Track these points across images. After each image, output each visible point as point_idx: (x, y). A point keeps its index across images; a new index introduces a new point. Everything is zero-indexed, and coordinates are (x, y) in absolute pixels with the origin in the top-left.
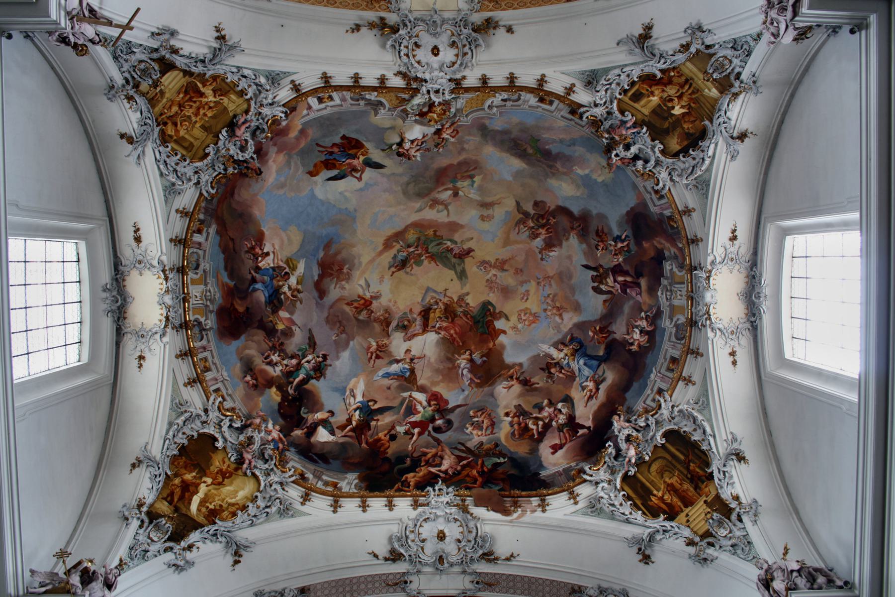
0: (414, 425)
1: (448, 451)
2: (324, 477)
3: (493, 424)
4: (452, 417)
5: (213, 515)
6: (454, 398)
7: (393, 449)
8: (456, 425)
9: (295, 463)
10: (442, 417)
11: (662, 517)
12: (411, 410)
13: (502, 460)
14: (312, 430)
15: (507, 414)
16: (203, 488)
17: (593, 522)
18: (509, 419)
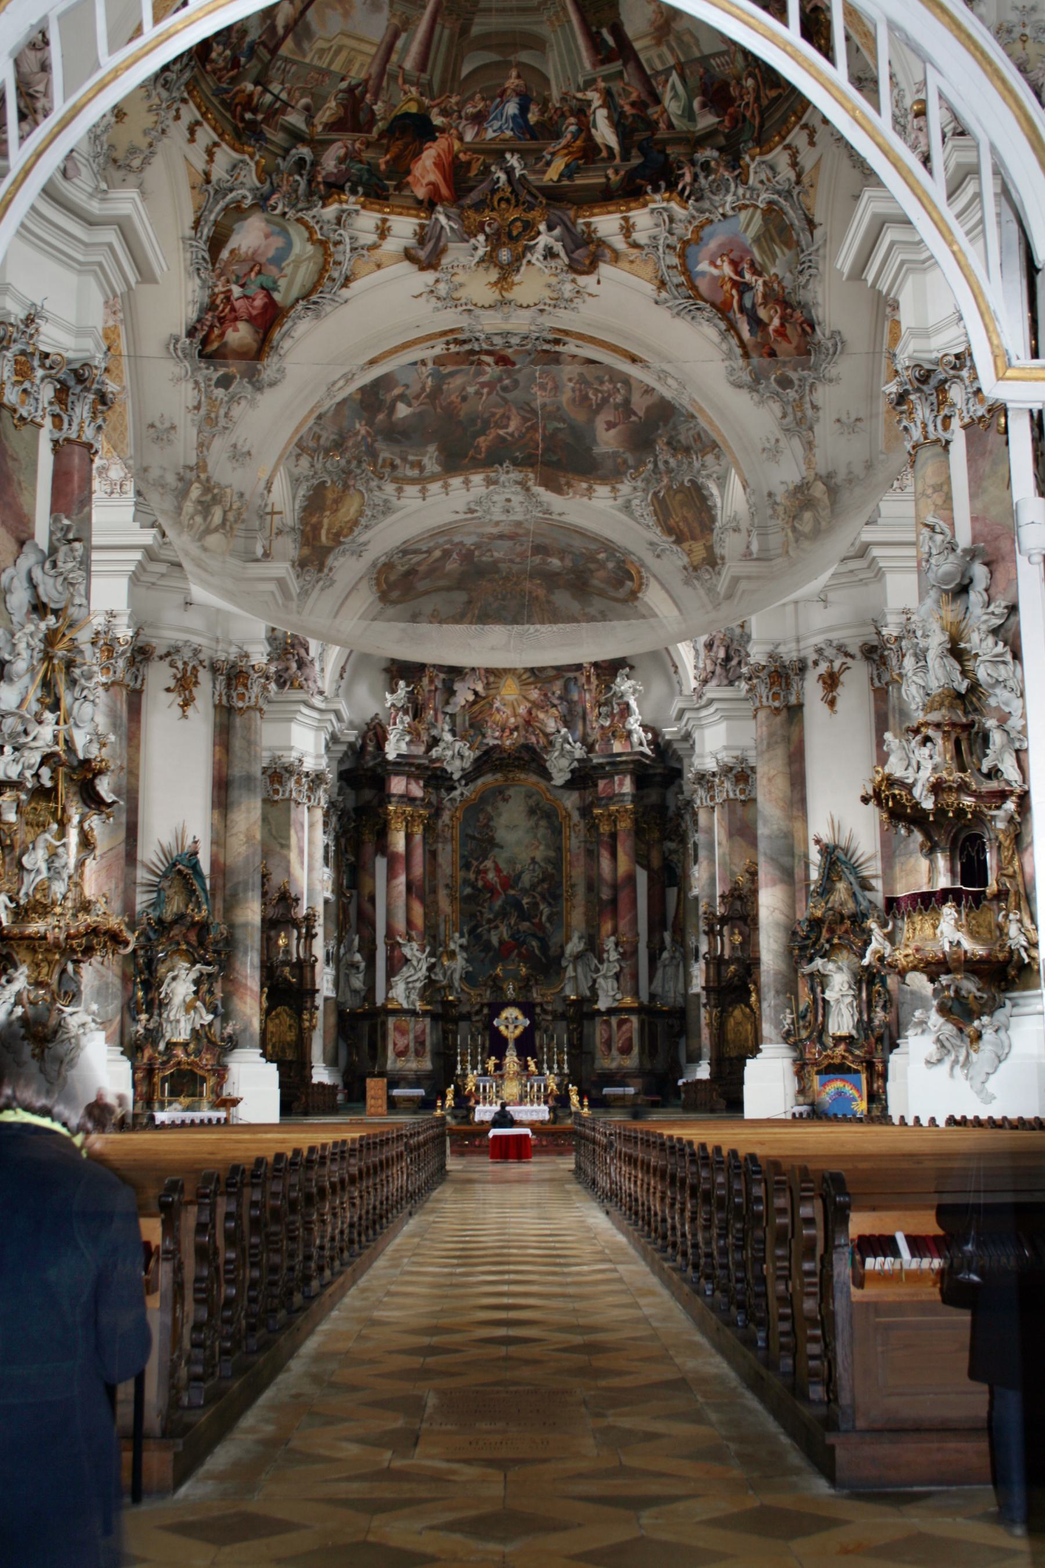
0: (483, 385)
1: (514, 411)
2: (411, 458)
5: (337, 537)
7: (464, 410)
8: (522, 384)
9: (385, 453)
10: (509, 376)
11: (673, 538)
13: (561, 425)
14: (392, 409)
15: (570, 380)
16: (326, 521)
17: (623, 517)
18: (571, 384)
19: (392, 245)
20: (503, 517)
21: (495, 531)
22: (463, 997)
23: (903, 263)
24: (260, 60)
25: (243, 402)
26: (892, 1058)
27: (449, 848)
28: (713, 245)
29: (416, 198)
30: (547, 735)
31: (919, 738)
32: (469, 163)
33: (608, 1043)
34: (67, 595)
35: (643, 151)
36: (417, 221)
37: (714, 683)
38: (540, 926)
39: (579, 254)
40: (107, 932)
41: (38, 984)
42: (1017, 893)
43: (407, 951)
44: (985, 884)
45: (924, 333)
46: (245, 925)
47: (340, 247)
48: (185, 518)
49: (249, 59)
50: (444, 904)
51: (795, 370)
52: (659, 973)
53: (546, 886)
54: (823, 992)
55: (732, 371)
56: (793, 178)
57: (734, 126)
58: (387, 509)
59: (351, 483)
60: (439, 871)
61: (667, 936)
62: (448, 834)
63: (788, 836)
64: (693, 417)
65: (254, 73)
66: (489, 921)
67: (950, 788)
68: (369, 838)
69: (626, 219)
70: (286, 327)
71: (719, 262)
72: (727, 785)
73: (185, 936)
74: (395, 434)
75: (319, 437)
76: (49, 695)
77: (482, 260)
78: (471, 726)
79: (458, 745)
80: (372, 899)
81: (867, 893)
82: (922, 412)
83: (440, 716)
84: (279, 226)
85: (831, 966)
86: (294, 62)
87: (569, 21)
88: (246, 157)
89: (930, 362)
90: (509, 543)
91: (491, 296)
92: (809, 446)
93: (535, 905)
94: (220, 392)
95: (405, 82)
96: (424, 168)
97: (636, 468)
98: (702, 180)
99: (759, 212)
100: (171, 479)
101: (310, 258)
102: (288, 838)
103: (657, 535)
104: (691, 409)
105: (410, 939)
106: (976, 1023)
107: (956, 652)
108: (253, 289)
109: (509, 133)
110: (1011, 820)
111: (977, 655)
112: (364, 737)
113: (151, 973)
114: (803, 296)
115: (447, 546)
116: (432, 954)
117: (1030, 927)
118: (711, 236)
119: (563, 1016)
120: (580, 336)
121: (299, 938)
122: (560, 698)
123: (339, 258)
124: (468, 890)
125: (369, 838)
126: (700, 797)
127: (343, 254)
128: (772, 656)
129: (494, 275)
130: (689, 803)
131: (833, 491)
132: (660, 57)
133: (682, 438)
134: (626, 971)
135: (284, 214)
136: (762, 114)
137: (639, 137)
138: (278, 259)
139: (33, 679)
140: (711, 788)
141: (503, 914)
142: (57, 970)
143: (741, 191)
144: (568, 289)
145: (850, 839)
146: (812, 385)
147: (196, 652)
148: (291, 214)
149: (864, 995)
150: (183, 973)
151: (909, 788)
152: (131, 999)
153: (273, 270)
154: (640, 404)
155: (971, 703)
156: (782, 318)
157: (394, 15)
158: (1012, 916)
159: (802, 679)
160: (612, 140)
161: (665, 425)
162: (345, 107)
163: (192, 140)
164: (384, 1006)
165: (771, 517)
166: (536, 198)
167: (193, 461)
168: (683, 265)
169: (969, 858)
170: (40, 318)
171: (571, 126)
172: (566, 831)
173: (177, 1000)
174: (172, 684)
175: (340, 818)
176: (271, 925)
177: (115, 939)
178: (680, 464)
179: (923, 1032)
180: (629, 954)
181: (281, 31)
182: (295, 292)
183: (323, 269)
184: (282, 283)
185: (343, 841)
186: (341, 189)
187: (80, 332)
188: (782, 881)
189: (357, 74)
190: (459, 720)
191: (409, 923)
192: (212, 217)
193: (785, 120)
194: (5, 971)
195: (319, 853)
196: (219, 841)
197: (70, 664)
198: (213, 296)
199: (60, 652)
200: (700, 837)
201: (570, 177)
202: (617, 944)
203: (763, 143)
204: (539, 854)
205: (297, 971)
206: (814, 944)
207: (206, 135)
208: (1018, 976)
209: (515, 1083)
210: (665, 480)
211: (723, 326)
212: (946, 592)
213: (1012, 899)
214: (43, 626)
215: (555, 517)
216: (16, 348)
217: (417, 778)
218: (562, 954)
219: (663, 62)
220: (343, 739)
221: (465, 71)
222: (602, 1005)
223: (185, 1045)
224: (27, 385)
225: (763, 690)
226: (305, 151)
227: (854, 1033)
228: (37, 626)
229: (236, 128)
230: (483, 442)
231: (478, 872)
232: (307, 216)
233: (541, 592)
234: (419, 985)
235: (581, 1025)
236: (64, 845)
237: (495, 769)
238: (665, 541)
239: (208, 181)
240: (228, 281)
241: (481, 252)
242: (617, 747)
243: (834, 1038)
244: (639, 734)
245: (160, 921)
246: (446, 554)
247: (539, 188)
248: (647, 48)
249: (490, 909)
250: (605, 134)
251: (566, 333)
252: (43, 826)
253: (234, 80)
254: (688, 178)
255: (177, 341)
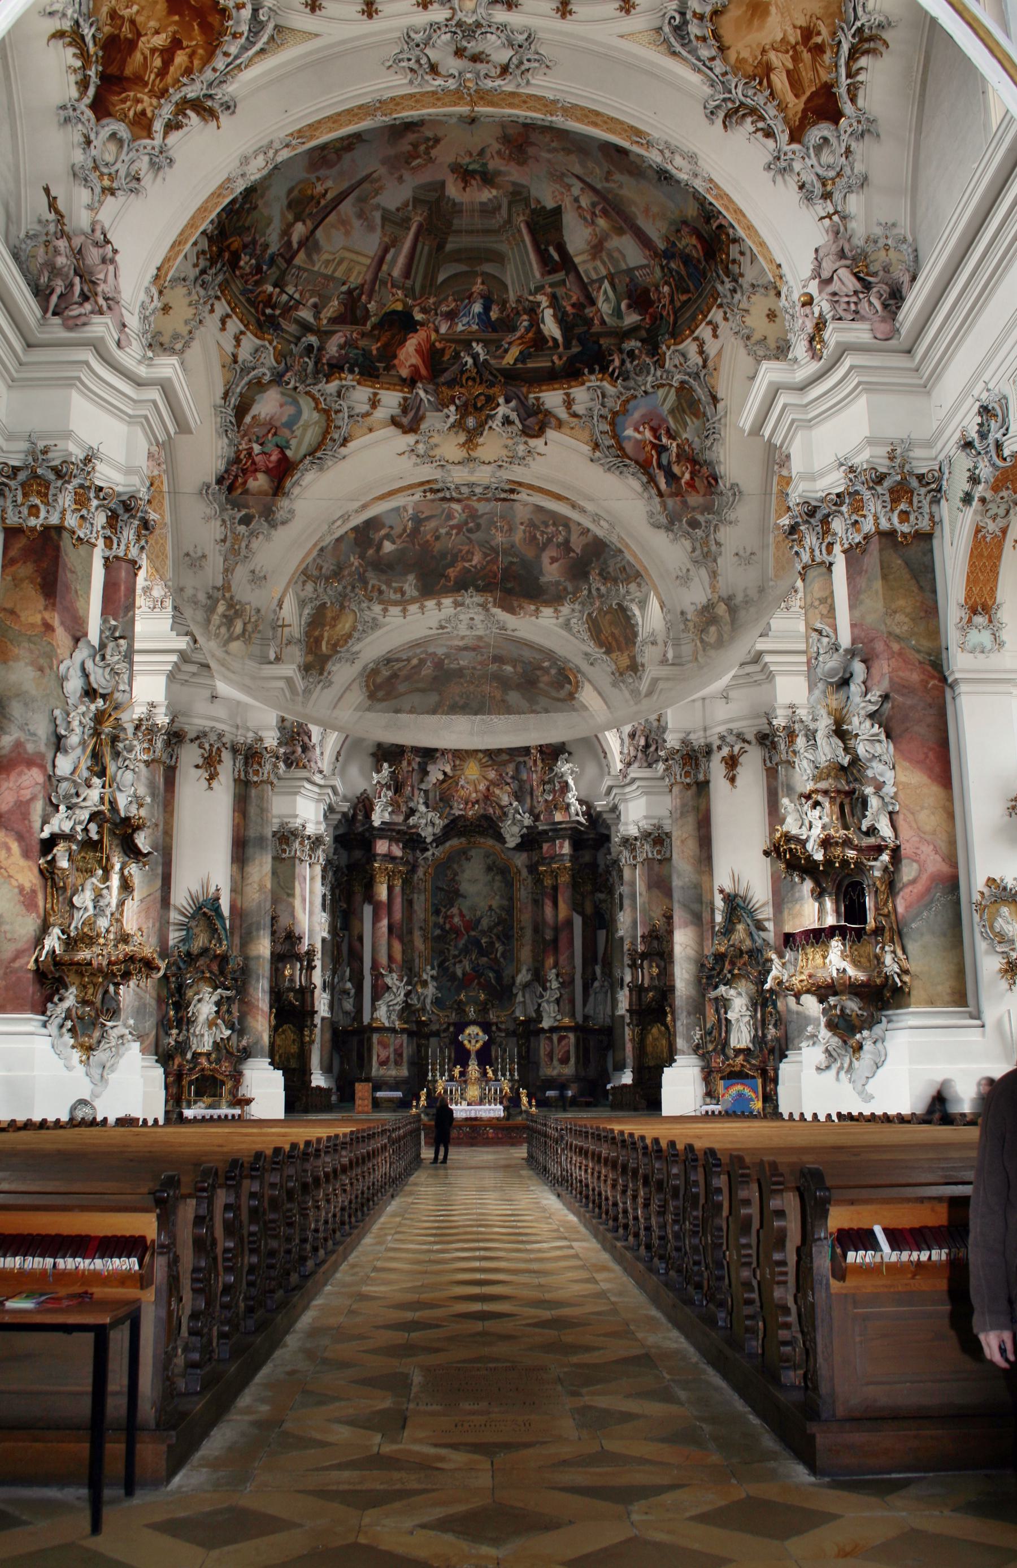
0: (452, 527)
3: (510, 530)
4: (481, 521)
5: (334, 647)
6: (482, 508)
7: (438, 547)
8: (483, 527)
9: (373, 581)
12: (450, 516)
13: (515, 560)
14: (380, 546)
16: (326, 634)
17: (564, 633)
19: (381, 414)
20: (468, 633)
21: (461, 643)
22: (434, 1018)
23: (793, 421)
24: (278, 267)
25: (261, 537)
26: (782, 1066)
27: (422, 898)
28: (637, 415)
29: (400, 377)
30: (501, 807)
31: (810, 802)
32: (443, 350)
33: (550, 1056)
34: (113, 683)
35: (580, 341)
36: (401, 395)
37: (636, 765)
38: (496, 960)
39: (531, 421)
40: (141, 960)
41: (85, 1002)
42: (891, 929)
43: (388, 981)
44: (865, 922)
45: (812, 477)
46: (258, 957)
47: (340, 415)
48: (212, 628)
49: (270, 267)
50: (419, 943)
51: (702, 514)
52: (591, 999)
53: (500, 928)
54: (726, 1013)
55: (651, 514)
56: (700, 362)
57: (653, 322)
58: (375, 625)
59: (346, 604)
60: (415, 918)
61: (598, 970)
62: (422, 886)
63: (697, 887)
64: (621, 551)
65: (273, 278)
66: (455, 956)
67: (837, 843)
68: (358, 889)
69: (568, 395)
70: (295, 478)
71: (641, 429)
72: (647, 847)
73: (208, 966)
74: (385, 567)
75: (321, 568)
76: (97, 764)
77: (453, 426)
78: (441, 800)
79: (430, 815)
80: (361, 939)
81: (761, 933)
82: (810, 540)
83: (416, 792)
84: (292, 397)
85: (732, 992)
86: (306, 270)
87: (523, 241)
88: (267, 343)
89: (816, 500)
90: (473, 654)
91: (460, 454)
92: (714, 575)
93: (492, 944)
94: (242, 529)
95: (393, 286)
96: (407, 353)
97: (574, 594)
98: (628, 365)
99: (673, 390)
100: (202, 597)
101: (316, 423)
102: (293, 888)
103: (591, 647)
104: (619, 545)
105: (391, 971)
106: (858, 1036)
107: (840, 732)
108: (270, 447)
109: (475, 327)
110: (885, 869)
111: (857, 735)
112: (355, 808)
113: (180, 996)
114: (708, 455)
115: (423, 656)
116: (408, 983)
117: (903, 957)
118: (636, 408)
119: (513, 1033)
120: (531, 487)
121: (301, 970)
122: (512, 778)
123: (339, 423)
124: (438, 932)
125: (358, 889)
126: (625, 857)
127: (342, 420)
128: (684, 742)
129: (462, 438)
130: (616, 862)
131: (733, 610)
132: (595, 269)
133: (611, 570)
134: (565, 997)
135: (296, 388)
136: (675, 314)
137: (578, 330)
138: (290, 424)
139: (84, 750)
140: (634, 850)
141: (466, 951)
142: (101, 991)
143: (659, 373)
144: (521, 449)
145: (748, 889)
146: (716, 526)
147: (220, 736)
148: (301, 388)
149: (759, 1015)
150: (207, 995)
151: (803, 843)
152: (164, 1017)
153: (286, 432)
154: (577, 543)
155: (852, 774)
156: (691, 473)
157: (385, 235)
158: (887, 948)
159: (709, 761)
160: (557, 334)
161: (598, 560)
162: (345, 305)
163: (223, 329)
164: (370, 1024)
165: (683, 631)
166: (496, 377)
167: (219, 583)
168: (613, 431)
169: (851, 900)
170: (97, 458)
171: (524, 322)
172: (517, 885)
173: (202, 1018)
174: (200, 762)
175: (335, 873)
176: (279, 959)
177: (149, 965)
178: (609, 591)
179: (814, 1044)
180: (567, 984)
181: (295, 245)
182: (303, 450)
183: (326, 432)
184: (293, 442)
185: (337, 891)
186: (341, 369)
187: (129, 471)
188: (692, 923)
189: (355, 280)
190: (431, 795)
191: (390, 958)
192: (238, 390)
193: (694, 318)
194: (57, 991)
195: (318, 901)
196: (237, 888)
197: (114, 739)
198: (238, 452)
199: (107, 729)
200: (625, 889)
201: (524, 362)
202: (557, 975)
203: (676, 335)
204: (495, 904)
205: (299, 996)
206: (719, 974)
207: (234, 325)
208: (892, 997)
209: (476, 1087)
210: (597, 604)
211: (645, 479)
212: (831, 684)
213: (887, 934)
214: (93, 707)
215: (509, 632)
216: (75, 482)
217: (397, 841)
218: (514, 983)
219: (597, 273)
220: (338, 809)
221: (440, 279)
222: (546, 1024)
223: (208, 1055)
224: (84, 512)
225: (677, 769)
226: (313, 339)
227: (751, 1046)
228: (88, 708)
229: (258, 321)
230: (452, 572)
231: (446, 917)
232: (314, 390)
233: (498, 694)
234: (398, 1008)
235: (528, 1041)
236: (108, 887)
237: (460, 834)
238: (598, 652)
239: (235, 362)
240: (250, 441)
241: (452, 419)
242: (558, 817)
243: (734, 1050)
244: (575, 807)
245: (189, 954)
246: (422, 662)
247: (498, 370)
248: (584, 262)
249: (456, 946)
250: (551, 328)
251: (520, 484)
252: (91, 872)
253: (257, 283)
254: (617, 363)
255: (208, 487)
